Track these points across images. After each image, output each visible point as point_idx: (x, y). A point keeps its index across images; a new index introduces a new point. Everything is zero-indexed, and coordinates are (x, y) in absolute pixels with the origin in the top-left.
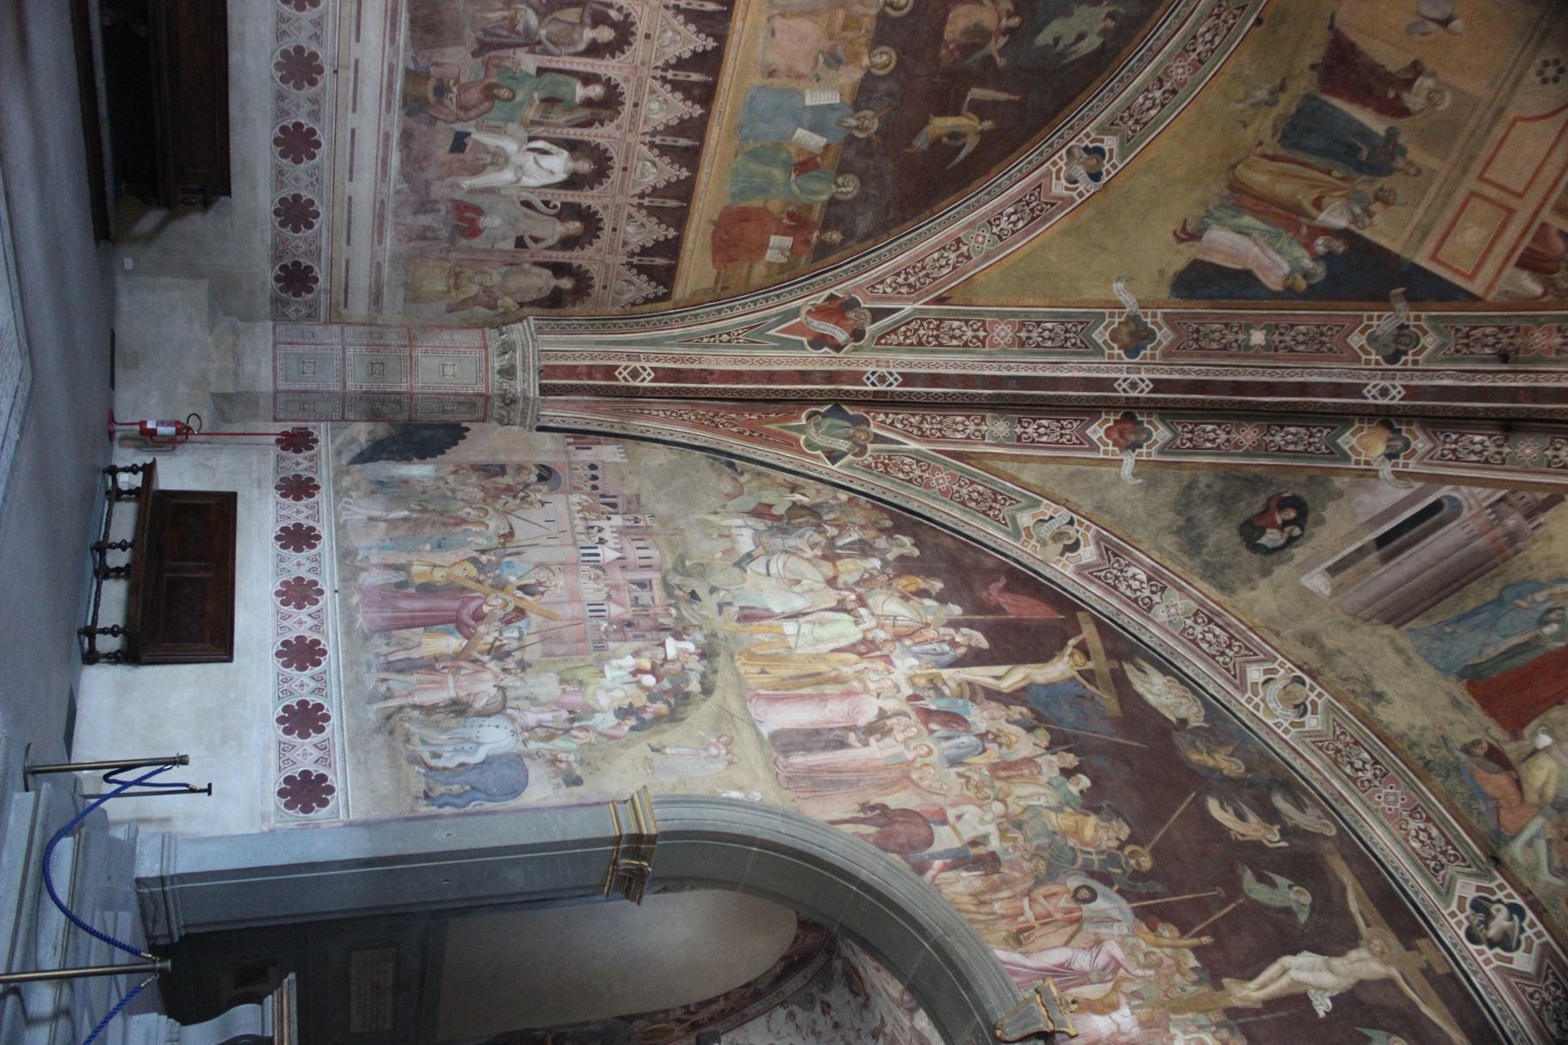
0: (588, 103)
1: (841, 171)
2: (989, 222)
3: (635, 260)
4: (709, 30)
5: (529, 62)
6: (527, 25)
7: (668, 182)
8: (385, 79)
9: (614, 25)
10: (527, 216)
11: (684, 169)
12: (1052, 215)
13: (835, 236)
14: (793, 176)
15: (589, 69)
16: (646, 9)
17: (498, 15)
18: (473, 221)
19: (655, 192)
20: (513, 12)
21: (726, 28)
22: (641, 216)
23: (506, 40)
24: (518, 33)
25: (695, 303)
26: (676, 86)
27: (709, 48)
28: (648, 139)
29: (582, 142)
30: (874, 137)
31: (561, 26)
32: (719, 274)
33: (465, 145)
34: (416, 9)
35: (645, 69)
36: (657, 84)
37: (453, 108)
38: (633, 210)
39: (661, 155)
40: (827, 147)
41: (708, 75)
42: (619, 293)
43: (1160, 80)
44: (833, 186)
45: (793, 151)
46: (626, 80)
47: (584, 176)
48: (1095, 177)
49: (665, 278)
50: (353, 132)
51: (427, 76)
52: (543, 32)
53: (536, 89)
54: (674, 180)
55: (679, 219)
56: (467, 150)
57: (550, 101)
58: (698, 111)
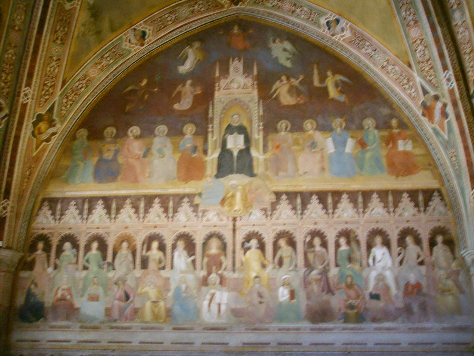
0: (348, 243)
1: (361, 128)
2: (371, 57)
3: (422, 209)
5: (334, 272)
10: (406, 262)
12: (359, 32)
13: (394, 122)
14: (368, 148)
18: (414, 287)
19: (386, 206)
22: (399, 211)
24: (322, 277)
25: (440, 177)
26: (335, 207)
30: (344, 118)
32: (422, 169)
36: (336, 215)
37: (359, 301)
38: (397, 214)
40: (352, 137)
42: (441, 213)
43: (293, 12)
44: (370, 129)
45: (356, 151)
46: (335, 229)
48: (337, 21)
49: (429, 194)
50: (377, 344)
55: (397, 194)
57: (350, 260)
58: (345, 196)
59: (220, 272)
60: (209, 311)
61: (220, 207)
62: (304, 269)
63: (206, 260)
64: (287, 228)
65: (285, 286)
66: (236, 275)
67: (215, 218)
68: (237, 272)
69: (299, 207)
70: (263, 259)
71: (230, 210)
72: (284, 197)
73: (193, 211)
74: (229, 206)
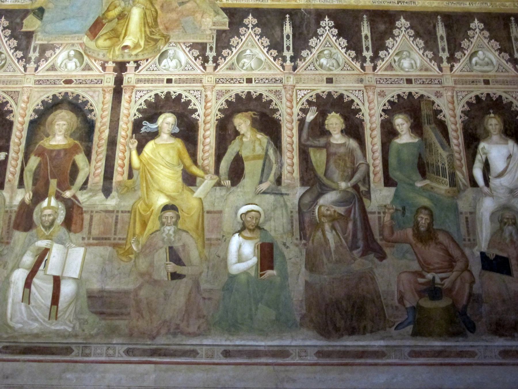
4: (313, 26)
6: (337, 203)
7: (491, 38)
8: (432, 361)
9: (323, 114)
11: (472, 25)
15: (377, 133)
16: (298, 86)
17: (330, 236)
20: (323, 219)
21: (309, 12)
23: (359, 223)
24: (349, 212)
27: (332, 23)
28: (445, 65)
29: (465, 130)
31: (332, 166)
33: (497, 257)
34: (337, 330)
35: (366, 78)
36: (380, 64)
37: (454, 275)
39: (462, 49)
41: (362, 20)
46: (382, 94)
47: (505, 122)
51: (417, 309)
52: (343, 185)
53: (412, 185)
54: (487, 34)
56: (505, 255)
58: (402, 22)
59: (68, 194)
60: (27, 297)
61: (85, 39)
62: (300, 191)
63: (34, 162)
64: (256, 89)
65: (246, 233)
66: (112, 202)
67: (71, 65)
68: (114, 193)
69: (288, 43)
70: (188, 161)
71: (110, 48)
72: (250, 20)
73: (16, 49)
74: (110, 39)
